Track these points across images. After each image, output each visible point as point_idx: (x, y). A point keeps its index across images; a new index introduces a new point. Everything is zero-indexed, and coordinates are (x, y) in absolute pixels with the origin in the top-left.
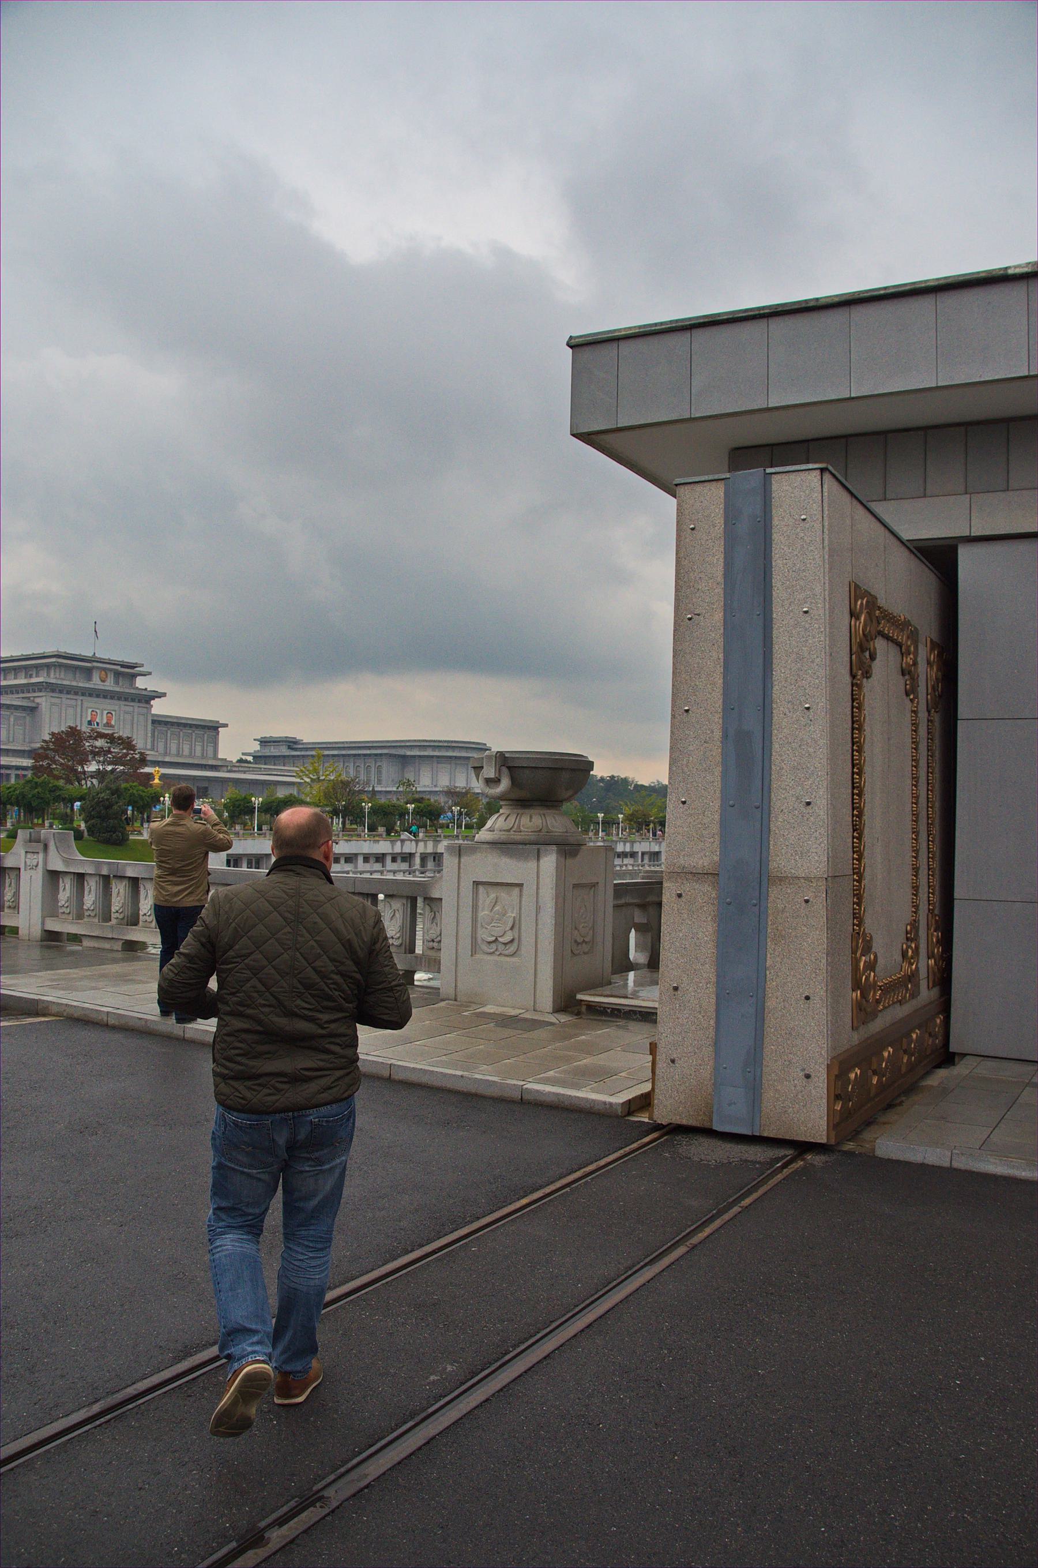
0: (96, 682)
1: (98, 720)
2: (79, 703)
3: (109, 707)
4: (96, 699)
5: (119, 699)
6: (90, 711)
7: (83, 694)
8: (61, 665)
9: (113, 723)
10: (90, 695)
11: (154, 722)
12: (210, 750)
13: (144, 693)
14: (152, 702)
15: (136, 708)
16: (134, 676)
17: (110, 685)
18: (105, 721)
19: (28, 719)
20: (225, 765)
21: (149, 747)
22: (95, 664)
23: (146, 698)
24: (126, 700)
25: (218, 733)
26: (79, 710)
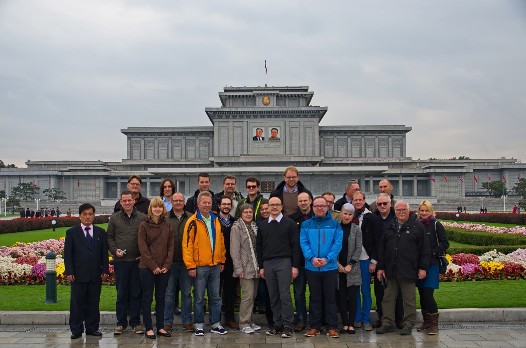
0: (259, 106)
1: (263, 136)
2: (245, 124)
3: (275, 124)
4: (261, 120)
6: (255, 129)
7: (248, 117)
8: (234, 97)
9: (278, 136)
11: (320, 132)
12: (397, 151)
15: (301, 122)
17: (273, 106)
18: (270, 136)
19: (211, 140)
20: (411, 163)
21: (317, 153)
22: (255, 92)
23: (321, 113)
25: (405, 137)
26: (245, 129)
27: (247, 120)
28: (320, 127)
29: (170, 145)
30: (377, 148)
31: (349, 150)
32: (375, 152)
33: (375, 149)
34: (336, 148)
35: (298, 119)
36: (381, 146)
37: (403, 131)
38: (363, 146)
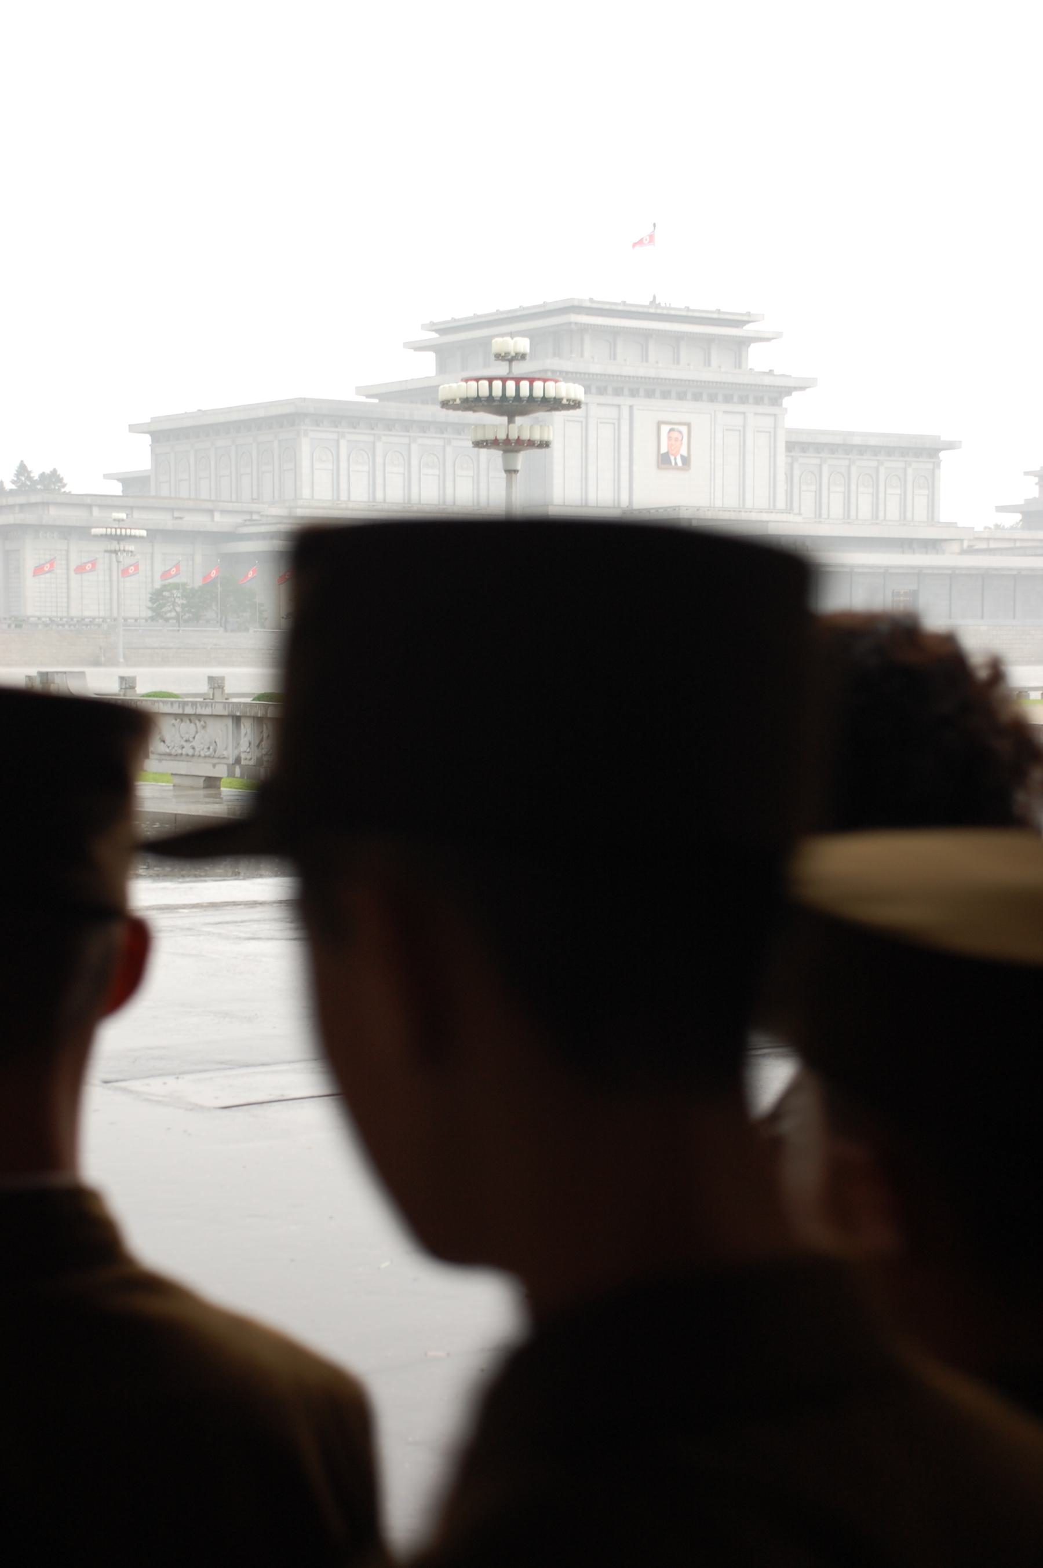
5: (712, 399)
7: (634, 393)
10: (650, 394)
11: (790, 446)
13: (767, 381)
14: (786, 401)
16: (742, 344)
21: (781, 504)
24: (728, 399)
25: (937, 465)
27: (630, 401)
28: (790, 431)
29: (414, 462)
30: (881, 495)
31: (824, 500)
32: (877, 504)
33: (877, 498)
34: (796, 491)
35: (741, 408)
36: (889, 491)
37: (926, 452)
38: (853, 487)
